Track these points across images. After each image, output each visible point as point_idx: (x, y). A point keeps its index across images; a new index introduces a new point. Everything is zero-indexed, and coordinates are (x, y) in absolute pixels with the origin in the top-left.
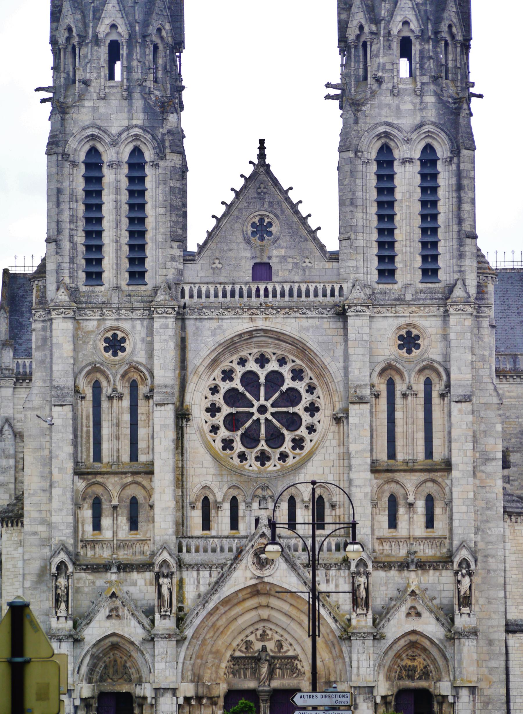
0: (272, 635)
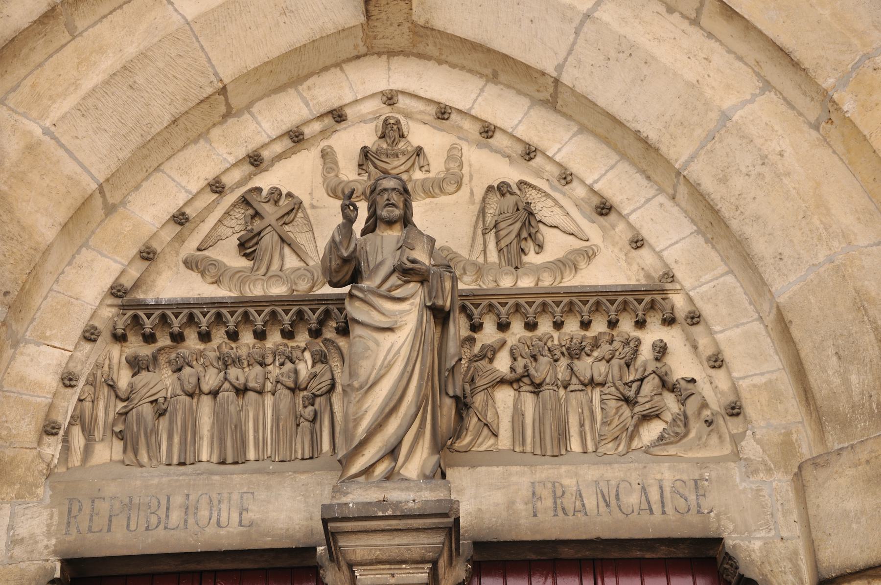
0: (454, 156)
